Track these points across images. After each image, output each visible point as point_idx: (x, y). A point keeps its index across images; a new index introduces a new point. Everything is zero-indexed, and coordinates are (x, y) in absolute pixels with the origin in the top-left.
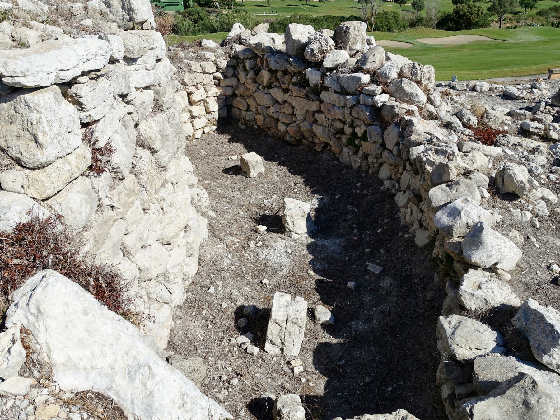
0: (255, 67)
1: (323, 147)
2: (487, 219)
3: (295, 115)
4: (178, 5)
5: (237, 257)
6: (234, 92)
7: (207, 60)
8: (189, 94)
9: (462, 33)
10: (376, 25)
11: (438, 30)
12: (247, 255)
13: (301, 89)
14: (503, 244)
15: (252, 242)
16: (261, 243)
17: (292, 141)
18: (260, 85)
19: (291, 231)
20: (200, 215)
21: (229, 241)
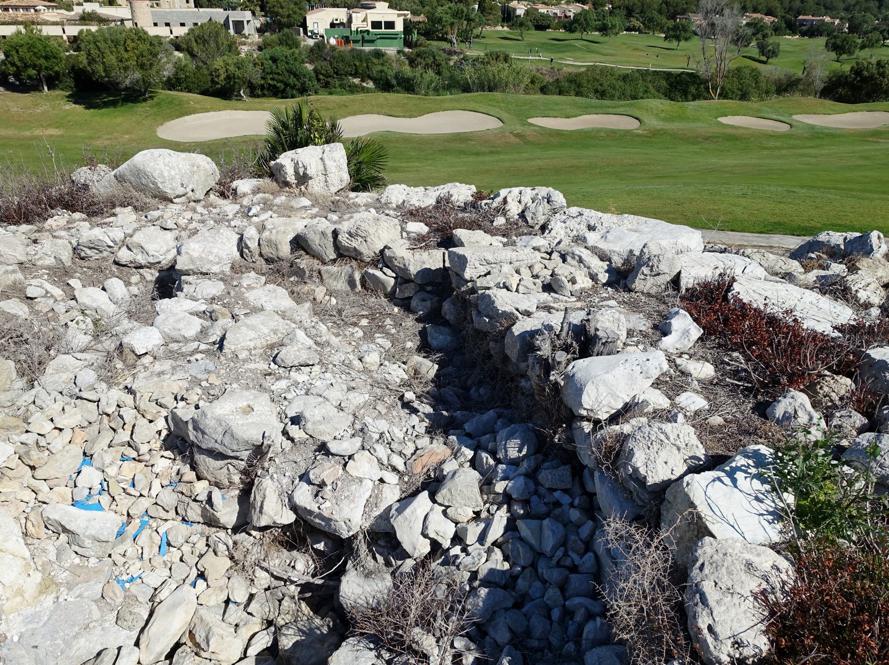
4: (396, 38)
9: (868, 108)
10: (723, 88)
11: (822, 100)
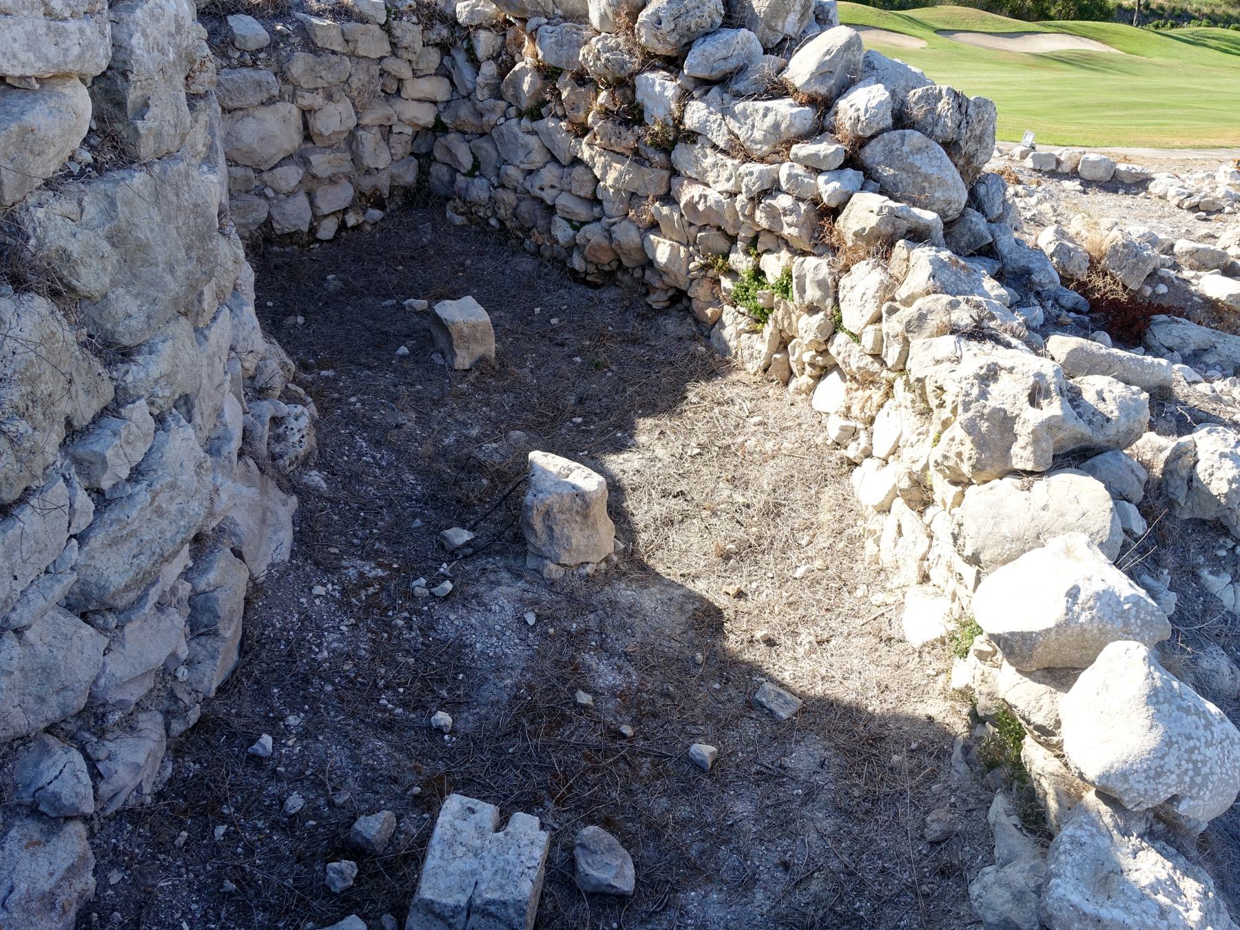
0: (499, 55)
1: (670, 299)
2: (1145, 623)
3: (599, 202)
5: (369, 630)
6: (438, 118)
7: (363, 20)
8: (306, 113)
12: (400, 623)
13: (623, 129)
14: (1201, 732)
15: (423, 581)
16: (448, 586)
17: (586, 273)
18: (510, 105)
19: (543, 557)
20: (272, 484)
21: (352, 572)
